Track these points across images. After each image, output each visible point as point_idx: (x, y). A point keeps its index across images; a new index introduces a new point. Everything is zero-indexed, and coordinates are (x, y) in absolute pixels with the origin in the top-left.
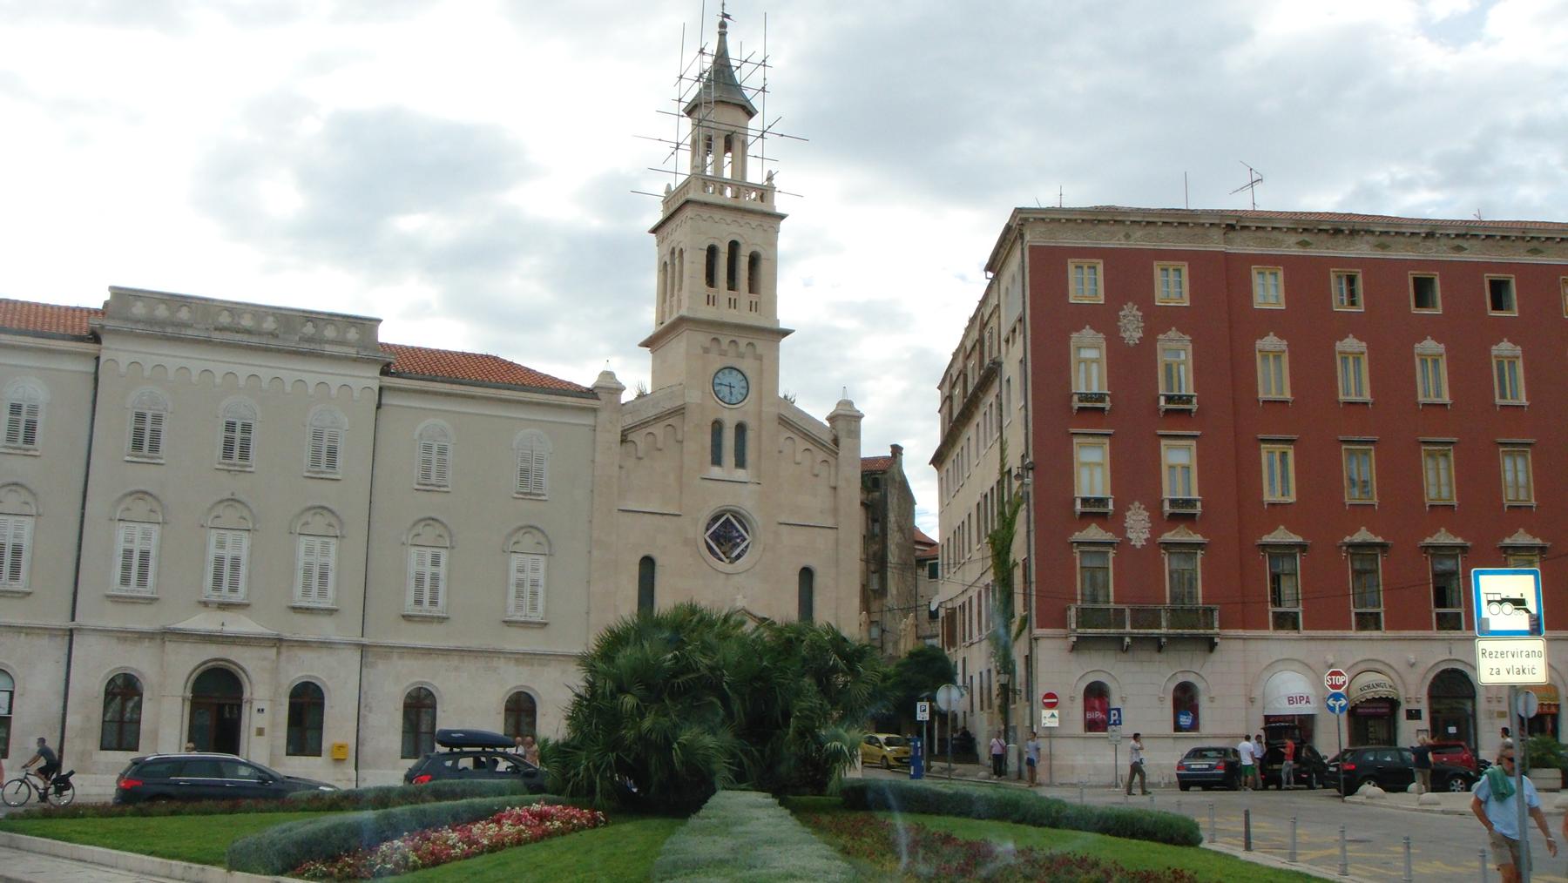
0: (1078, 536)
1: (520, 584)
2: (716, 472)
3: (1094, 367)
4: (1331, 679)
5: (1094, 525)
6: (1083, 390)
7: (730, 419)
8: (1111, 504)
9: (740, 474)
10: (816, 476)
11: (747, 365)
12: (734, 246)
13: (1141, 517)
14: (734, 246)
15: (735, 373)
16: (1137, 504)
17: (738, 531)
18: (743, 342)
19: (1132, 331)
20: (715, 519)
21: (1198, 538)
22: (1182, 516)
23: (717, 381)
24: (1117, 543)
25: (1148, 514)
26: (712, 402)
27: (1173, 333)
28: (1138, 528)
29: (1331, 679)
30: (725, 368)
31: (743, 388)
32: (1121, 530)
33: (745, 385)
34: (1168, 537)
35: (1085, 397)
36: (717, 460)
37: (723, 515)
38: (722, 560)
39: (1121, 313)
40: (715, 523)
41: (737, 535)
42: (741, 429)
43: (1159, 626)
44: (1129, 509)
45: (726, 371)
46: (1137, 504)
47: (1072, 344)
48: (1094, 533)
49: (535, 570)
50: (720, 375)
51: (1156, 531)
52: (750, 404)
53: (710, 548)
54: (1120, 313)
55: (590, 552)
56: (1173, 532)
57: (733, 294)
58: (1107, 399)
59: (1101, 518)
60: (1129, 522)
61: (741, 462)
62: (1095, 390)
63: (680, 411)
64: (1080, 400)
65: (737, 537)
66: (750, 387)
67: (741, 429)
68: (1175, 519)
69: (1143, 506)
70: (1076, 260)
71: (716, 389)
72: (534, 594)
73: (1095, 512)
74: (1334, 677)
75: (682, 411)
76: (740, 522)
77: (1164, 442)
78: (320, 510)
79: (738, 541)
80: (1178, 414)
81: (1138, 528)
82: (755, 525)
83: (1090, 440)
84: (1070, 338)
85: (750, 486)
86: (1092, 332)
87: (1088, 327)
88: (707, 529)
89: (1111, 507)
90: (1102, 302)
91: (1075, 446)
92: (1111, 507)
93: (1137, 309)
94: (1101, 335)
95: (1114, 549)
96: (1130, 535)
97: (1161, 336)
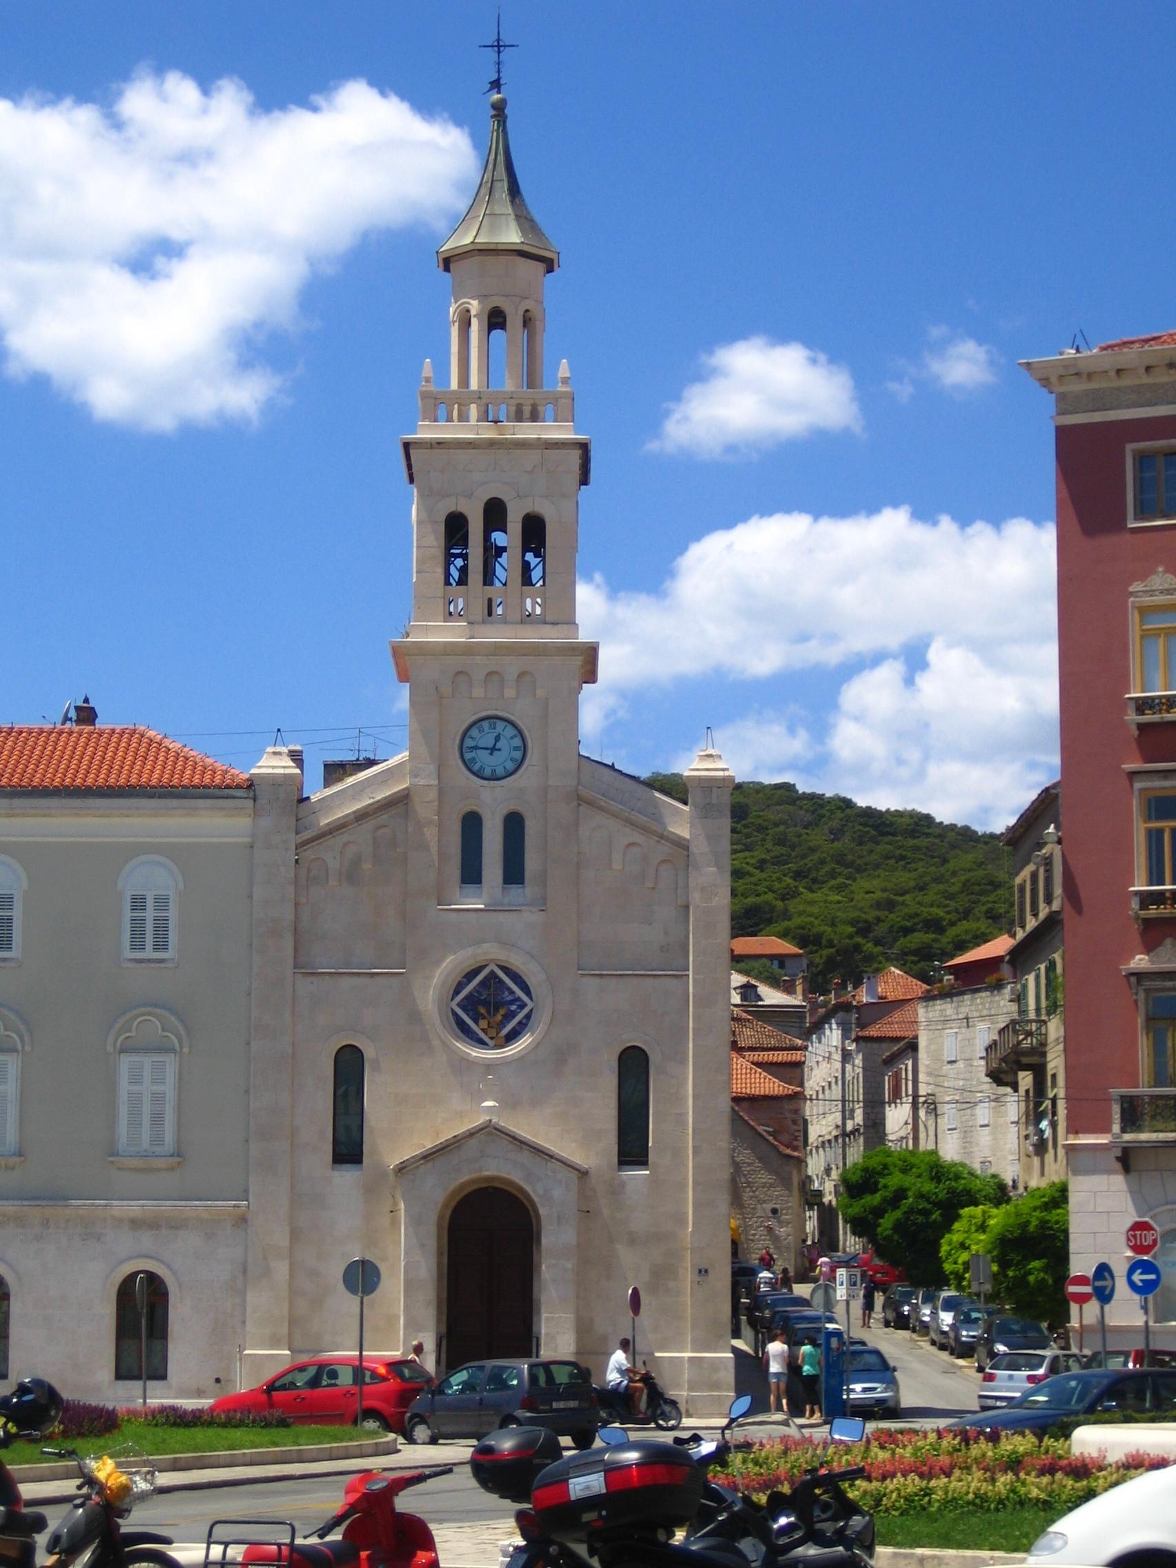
1: (135, 1100)
4: (1135, 1237)
11: (523, 713)
17: (512, 992)
23: (469, 742)
29: (1135, 1237)
31: (516, 748)
33: (514, 732)
36: (471, 874)
40: (469, 981)
41: (510, 998)
50: (474, 732)
52: (526, 778)
55: (248, 1044)
61: (514, 873)
63: (401, 802)
65: (512, 1002)
66: (530, 745)
71: (468, 756)
72: (157, 1119)
74: (1138, 1233)
79: (513, 1008)
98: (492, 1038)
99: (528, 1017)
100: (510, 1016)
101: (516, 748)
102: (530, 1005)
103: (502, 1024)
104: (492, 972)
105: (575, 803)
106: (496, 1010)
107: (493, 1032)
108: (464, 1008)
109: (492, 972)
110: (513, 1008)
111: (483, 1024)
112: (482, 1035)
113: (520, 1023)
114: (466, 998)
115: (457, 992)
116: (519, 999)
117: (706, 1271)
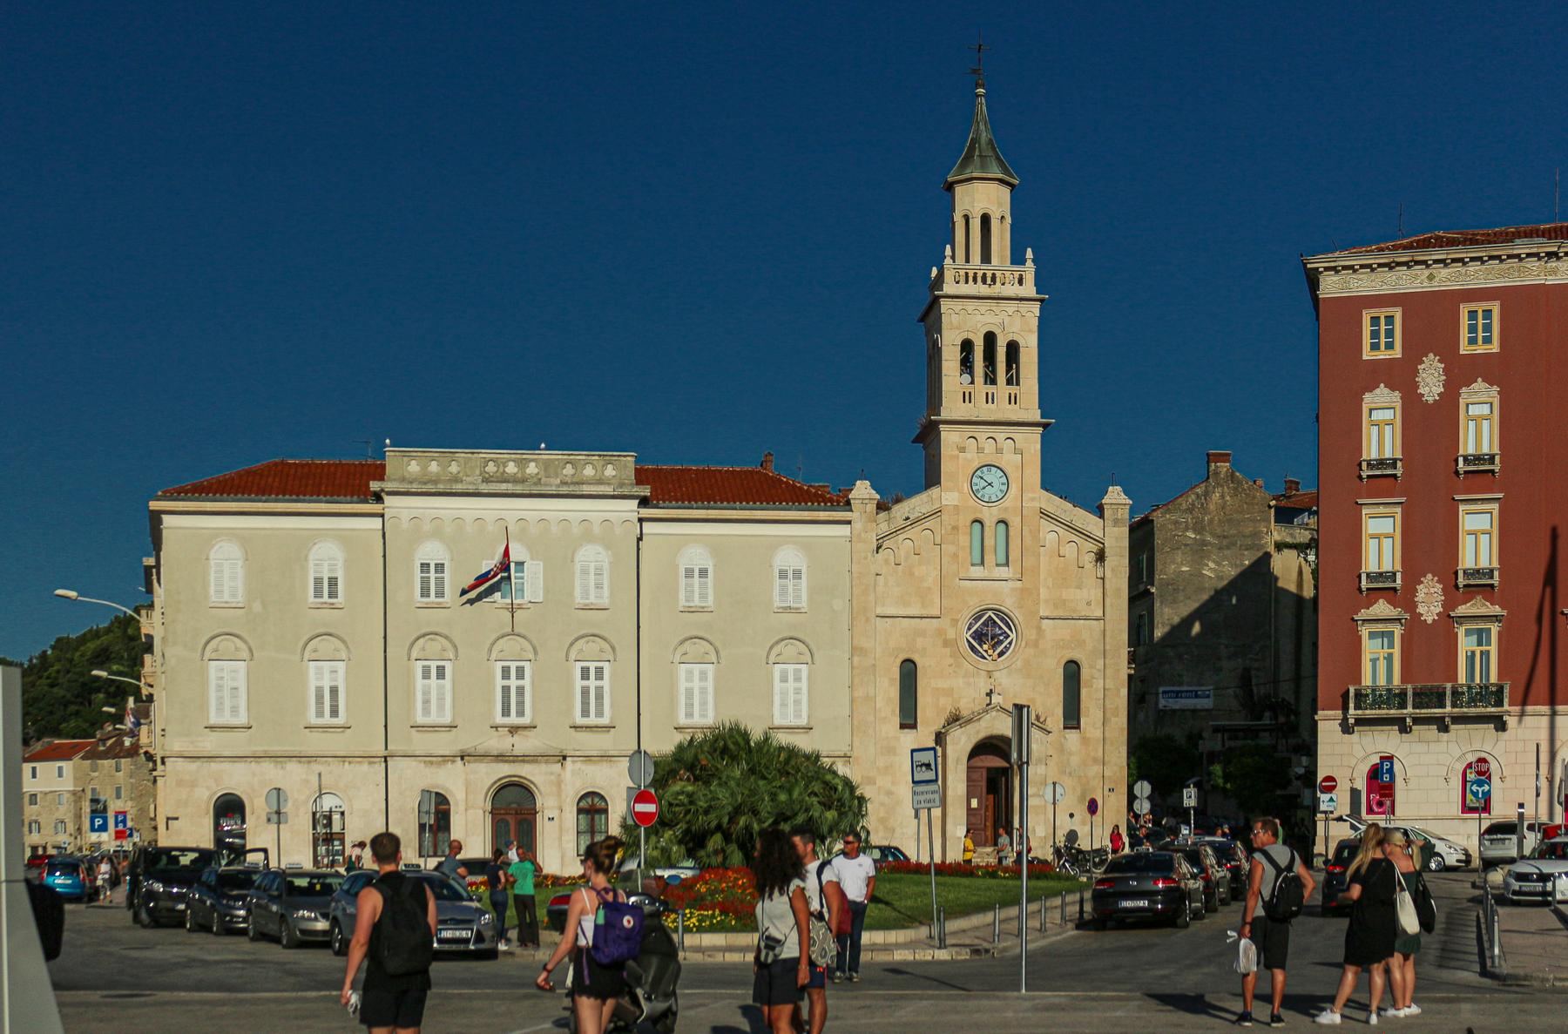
0: (1364, 614)
2: (977, 572)
3: (1388, 429)
5: (1381, 601)
6: (1374, 455)
8: (1399, 576)
9: (1003, 572)
12: (990, 339)
13: (1432, 590)
14: (990, 339)
16: (1429, 576)
19: (1431, 381)
20: (977, 619)
21: (1496, 610)
22: (1479, 586)
24: (1406, 619)
25: (1441, 586)
26: (972, 502)
27: (1479, 385)
28: (1429, 600)
32: (1410, 605)
34: (1462, 610)
35: (1381, 463)
37: (984, 614)
38: (985, 658)
39: (1423, 366)
43: (1443, 706)
44: (1422, 582)
46: (1429, 576)
47: (1364, 405)
48: (1382, 608)
49: (798, 679)
51: (1449, 604)
53: (972, 648)
54: (1419, 367)
56: (1468, 605)
57: (991, 389)
58: (1399, 464)
59: (1390, 593)
60: (1420, 596)
62: (1388, 454)
64: (1369, 464)
68: (1472, 591)
69: (1436, 578)
70: (1372, 310)
73: (1382, 587)
75: (939, 514)
76: (1002, 620)
77: (1462, 507)
78: (592, 638)
79: (1001, 638)
80: (1480, 475)
81: (1429, 600)
82: (1017, 622)
83: (1382, 509)
84: (1362, 400)
85: (1010, 584)
86: (1387, 391)
87: (1382, 385)
88: (969, 629)
89: (1399, 581)
90: (1399, 356)
91: (1364, 516)
92: (1399, 581)
93: (1439, 361)
94: (1397, 393)
95: (1402, 625)
96: (1421, 609)
97: (1464, 390)
99: (1010, 643)
100: (1001, 642)
101: (1003, 484)
102: (1013, 636)
104: (990, 616)
106: (992, 639)
107: (990, 652)
108: (973, 638)
110: (1001, 638)
111: (985, 647)
113: (1006, 647)
114: (974, 632)
115: (969, 629)
116: (1005, 632)
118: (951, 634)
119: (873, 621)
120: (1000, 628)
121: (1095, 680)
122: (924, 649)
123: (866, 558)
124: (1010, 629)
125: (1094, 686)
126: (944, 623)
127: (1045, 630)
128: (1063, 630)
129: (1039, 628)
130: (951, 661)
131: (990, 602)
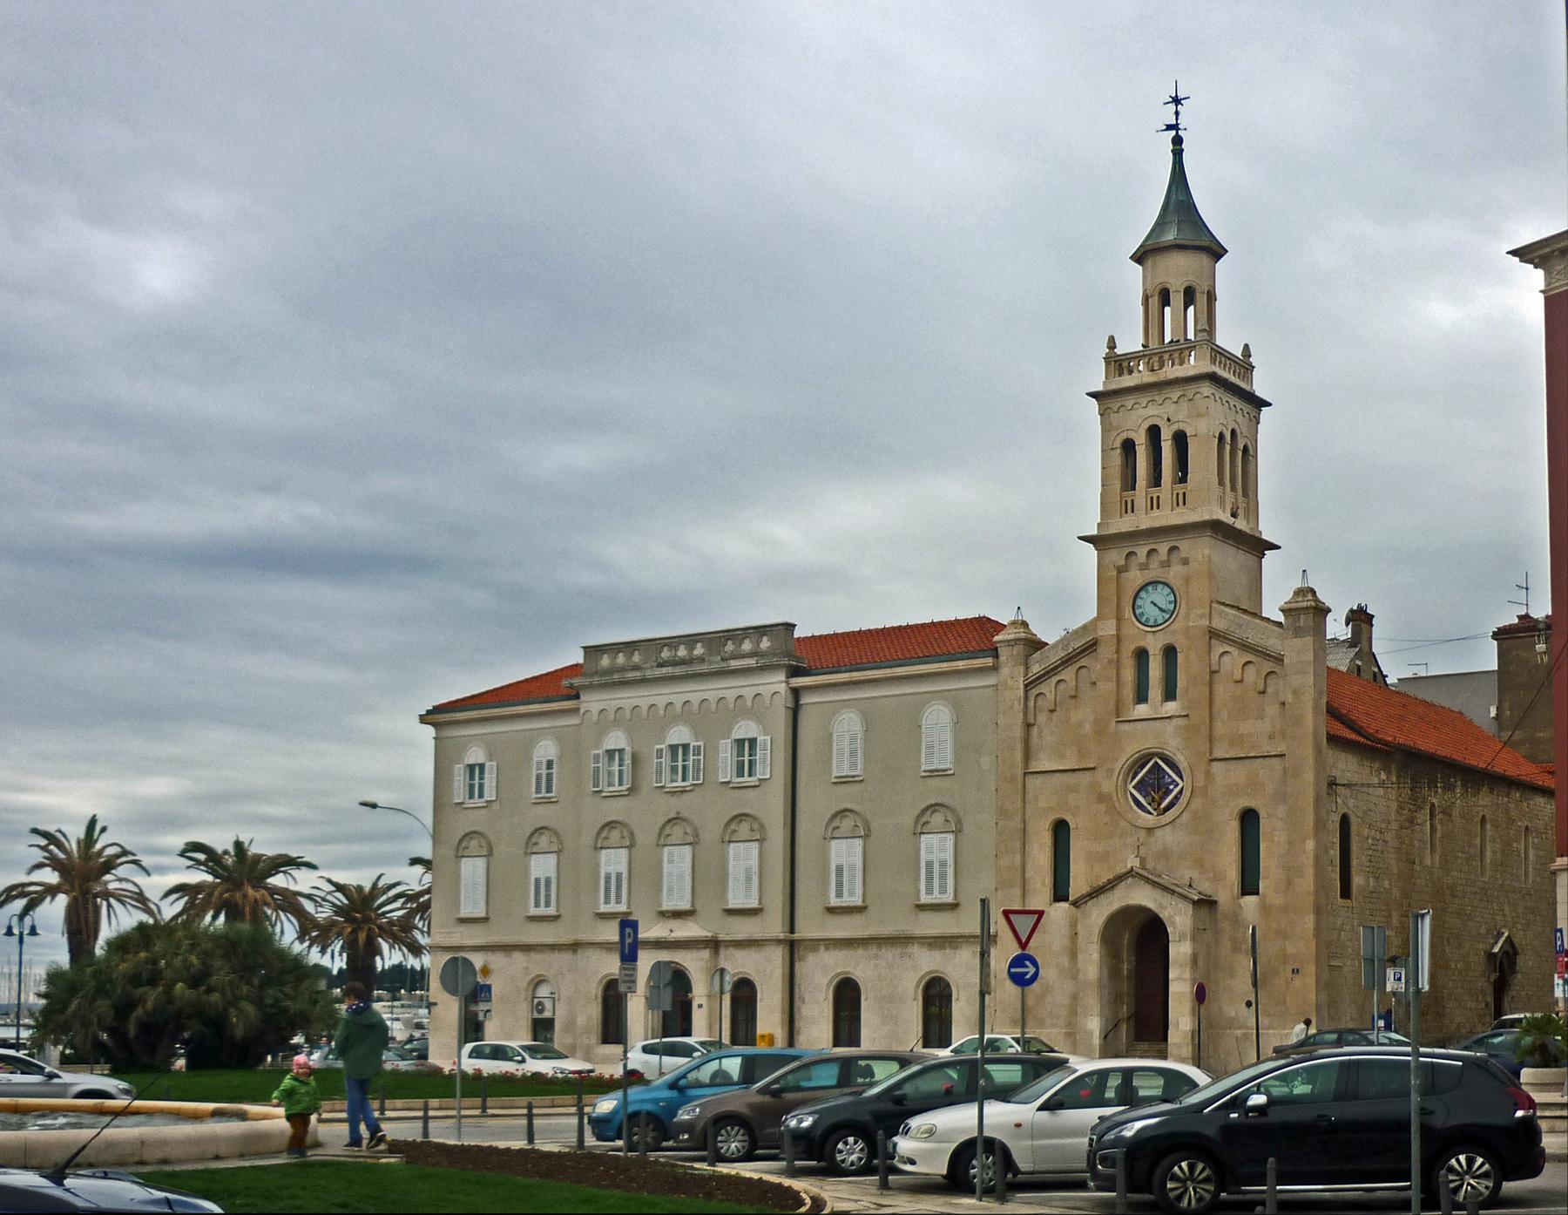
2: (1142, 710)
7: (1155, 646)
9: (1171, 707)
10: (1264, 692)
15: (1160, 587)
18: (1163, 548)
30: (1147, 585)
31: (1170, 602)
36: (1141, 697)
42: (1170, 653)
45: (1150, 588)
63: (1091, 647)
67: (1170, 653)
98: (1155, 810)
99: (1181, 792)
100: (1168, 792)
103: (1163, 798)
105: (1208, 637)
109: (1156, 762)
112: (1149, 808)
116: (1174, 781)
117: (1298, 970)
118: (1108, 786)
119: (1020, 779)
120: (1170, 776)
121: (1275, 832)
122: (1077, 807)
123: (1011, 707)
124: (1181, 777)
125: (1276, 840)
126: (1100, 775)
127: (1214, 774)
128: (1239, 772)
129: (1208, 773)
130: (1106, 819)
131: (1150, 744)
